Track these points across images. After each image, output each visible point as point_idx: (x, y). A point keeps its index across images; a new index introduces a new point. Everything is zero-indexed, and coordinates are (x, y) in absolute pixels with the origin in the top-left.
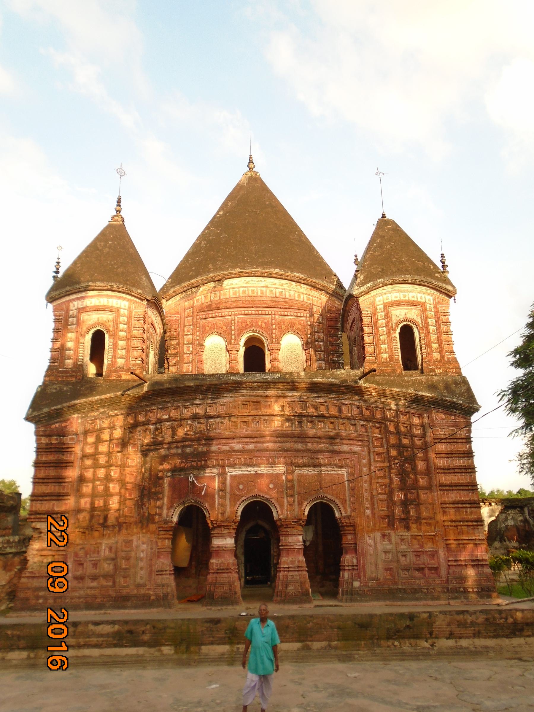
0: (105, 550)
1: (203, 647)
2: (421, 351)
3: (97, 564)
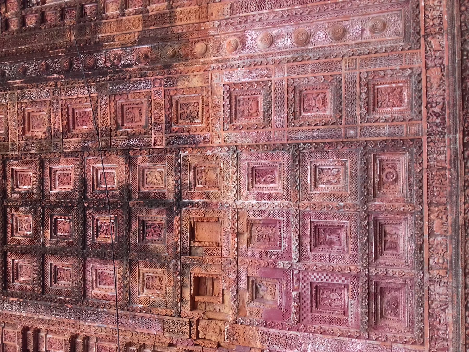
0: (261, 196)
3: (315, 228)
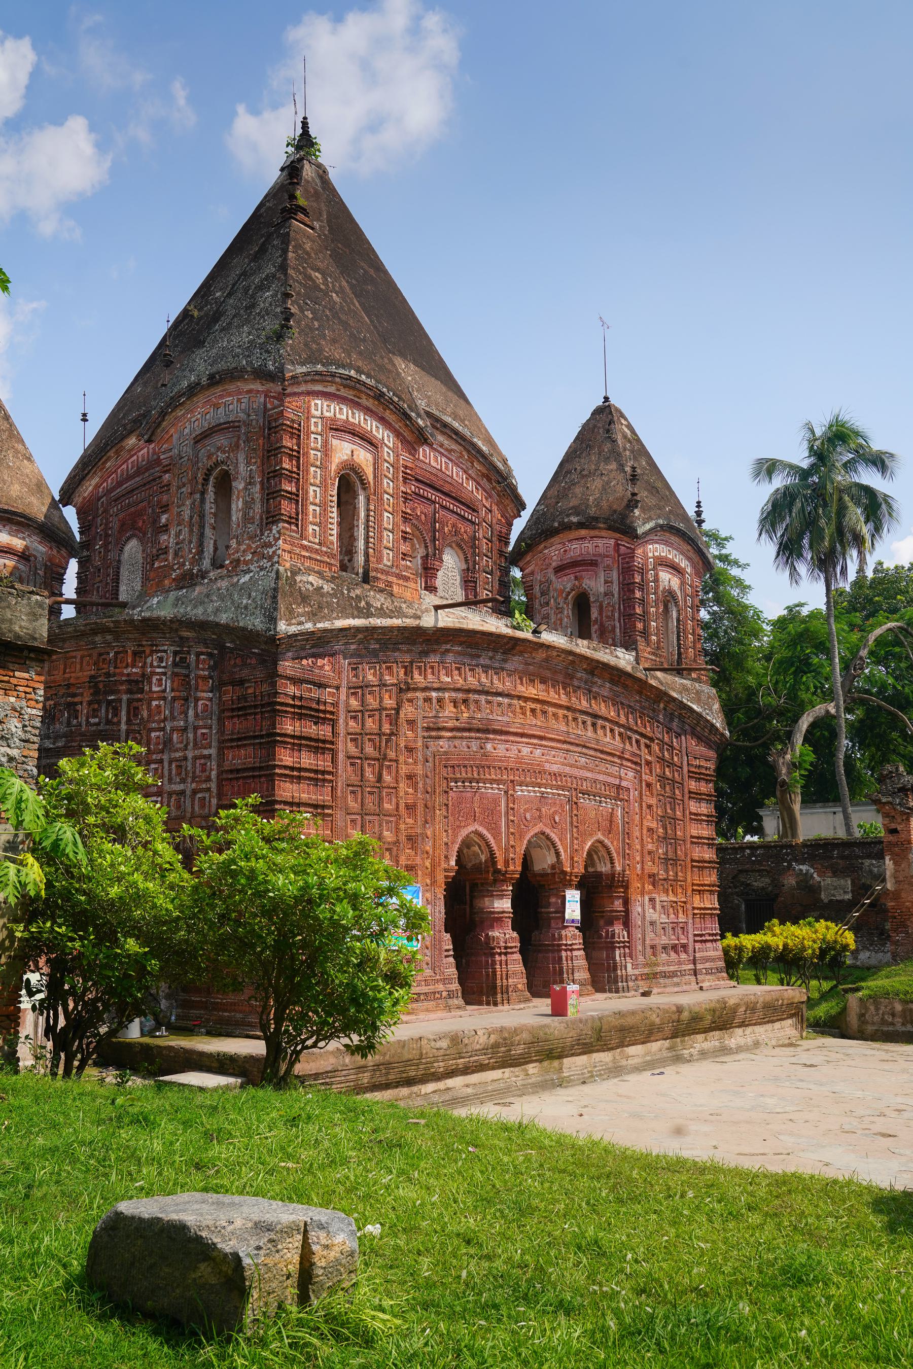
1: (565, 1060)
2: (679, 640)
